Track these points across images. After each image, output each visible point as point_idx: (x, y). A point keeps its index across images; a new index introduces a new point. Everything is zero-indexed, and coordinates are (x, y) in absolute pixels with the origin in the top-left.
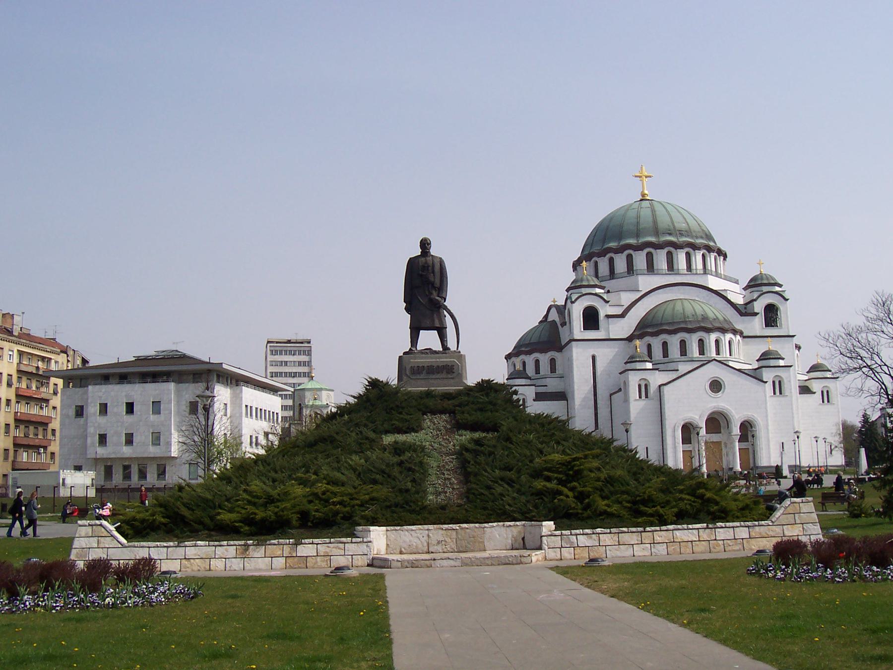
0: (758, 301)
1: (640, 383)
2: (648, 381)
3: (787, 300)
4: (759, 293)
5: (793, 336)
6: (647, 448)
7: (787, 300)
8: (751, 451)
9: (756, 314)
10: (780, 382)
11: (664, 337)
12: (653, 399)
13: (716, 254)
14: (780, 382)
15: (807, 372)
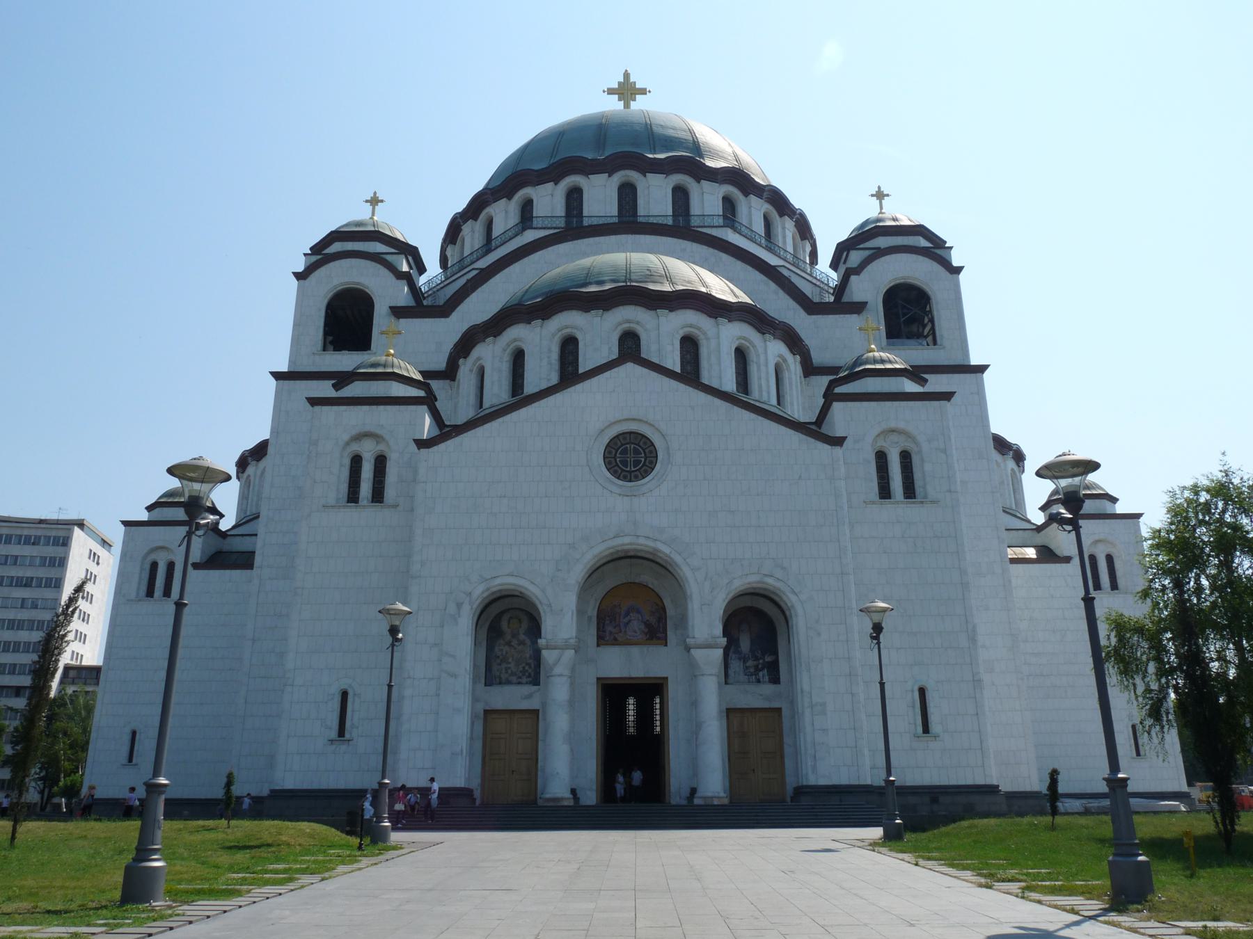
0: (862, 275)
1: (355, 448)
2: (387, 443)
3: (958, 270)
4: (867, 253)
5: (982, 369)
6: (344, 695)
7: (958, 270)
8: (786, 713)
9: (858, 308)
10: (906, 457)
11: (518, 333)
12: (395, 506)
13: (767, 207)
14: (906, 457)
15: (1043, 508)
